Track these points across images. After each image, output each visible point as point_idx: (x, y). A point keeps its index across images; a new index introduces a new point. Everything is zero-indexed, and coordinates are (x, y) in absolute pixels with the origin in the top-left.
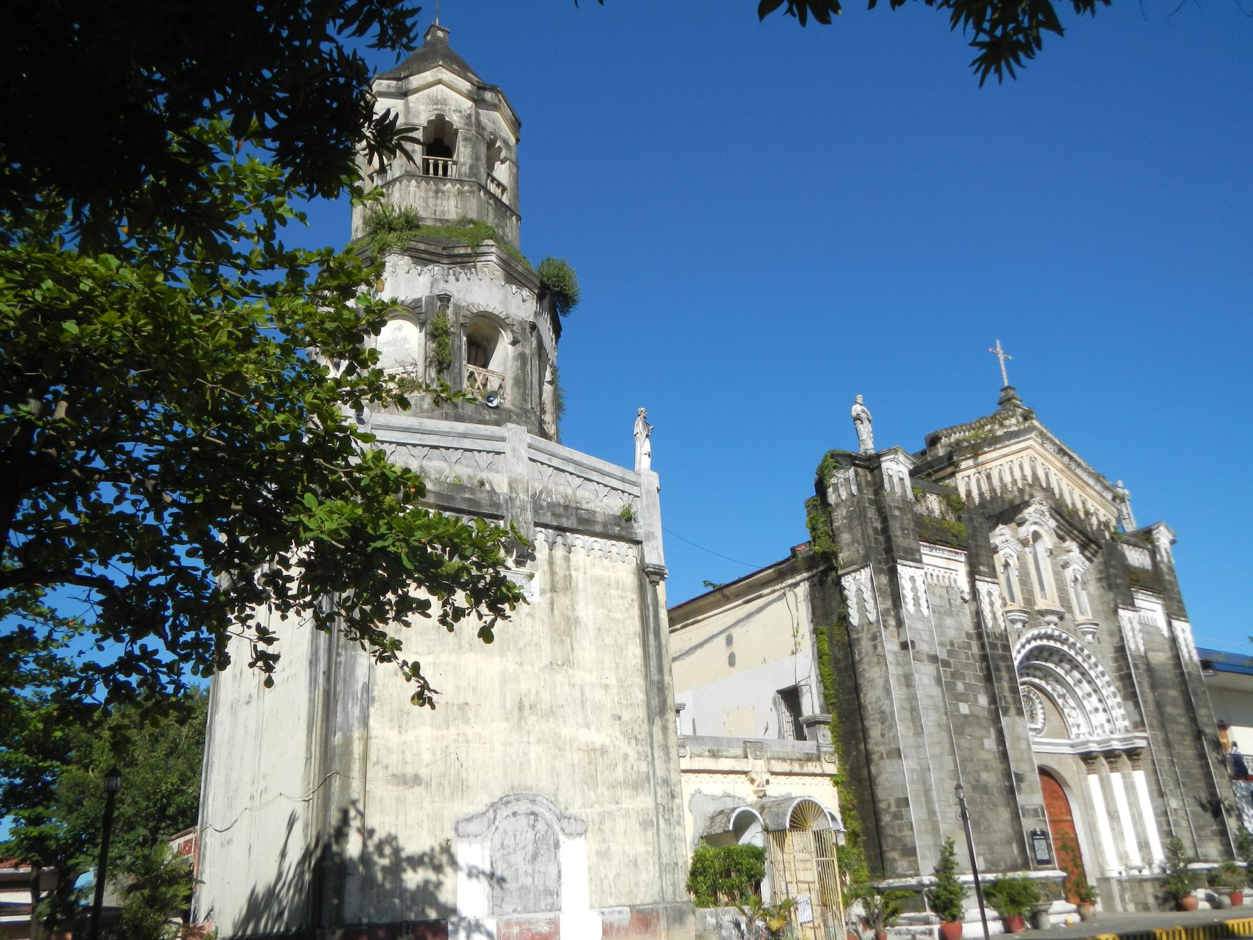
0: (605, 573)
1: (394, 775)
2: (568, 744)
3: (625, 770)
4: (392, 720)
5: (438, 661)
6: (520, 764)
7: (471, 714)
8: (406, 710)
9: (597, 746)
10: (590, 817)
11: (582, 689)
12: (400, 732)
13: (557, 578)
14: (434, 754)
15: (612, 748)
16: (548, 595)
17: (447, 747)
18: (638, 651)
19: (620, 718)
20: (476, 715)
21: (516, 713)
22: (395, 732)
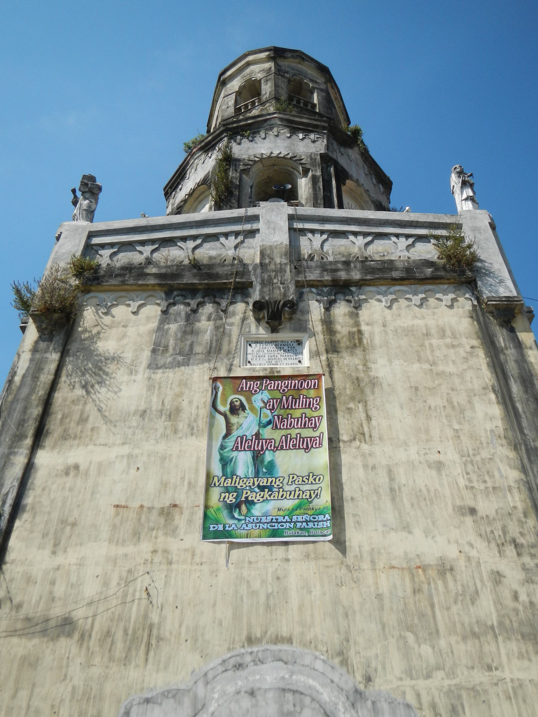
0: (416, 322)
1: (28, 619)
2: (367, 557)
3: (498, 602)
4: (45, 535)
5: (136, 451)
6: (268, 597)
7: (180, 521)
8: (71, 520)
9: (431, 559)
10: (425, 700)
11: (390, 472)
12: (54, 553)
13: (338, 336)
14: (106, 584)
15: (462, 563)
16: (324, 358)
17: (130, 571)
18: (497, 410)
19: (473, 511)
22: (47, 552)
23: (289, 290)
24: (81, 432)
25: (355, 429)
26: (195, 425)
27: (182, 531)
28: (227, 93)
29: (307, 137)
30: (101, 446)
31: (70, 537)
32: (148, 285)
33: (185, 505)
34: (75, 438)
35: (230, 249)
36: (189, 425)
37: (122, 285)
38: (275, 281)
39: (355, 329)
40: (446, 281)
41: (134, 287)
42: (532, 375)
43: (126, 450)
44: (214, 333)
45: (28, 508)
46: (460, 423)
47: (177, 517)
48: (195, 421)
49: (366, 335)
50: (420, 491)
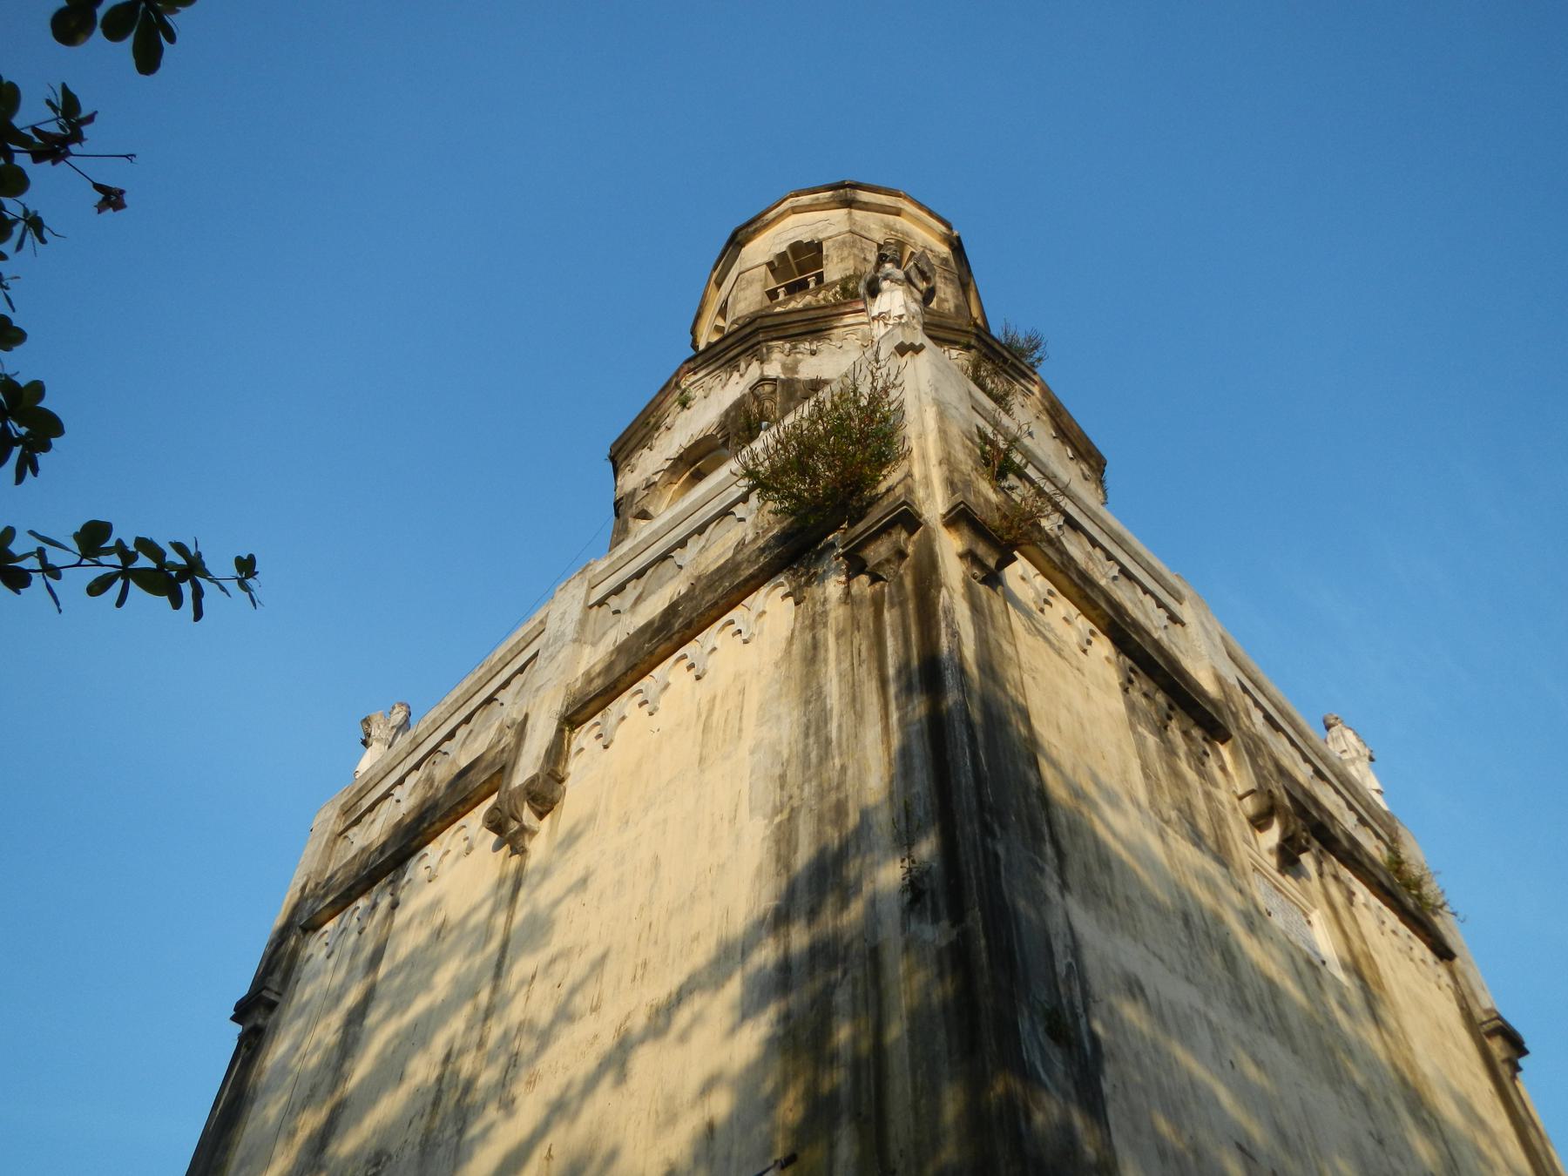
28: (857, 229)
37: (1061, 572)
41: (1072, 591)
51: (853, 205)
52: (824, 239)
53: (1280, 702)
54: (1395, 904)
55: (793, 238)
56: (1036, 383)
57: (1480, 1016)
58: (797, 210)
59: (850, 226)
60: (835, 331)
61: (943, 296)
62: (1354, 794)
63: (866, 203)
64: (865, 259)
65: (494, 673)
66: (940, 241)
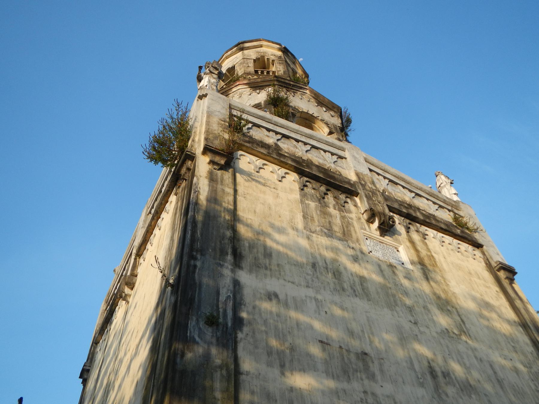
5: (319, 297)
11: (491, 366)
20: (382, 371)
21: (429, 377)
23: (385, 208)
24: (270, 264)
25: (459, 327)
26: (355, 289)
27: (379, 377)
28: (245, 57)
29: (328, 111)
30: (290, 283)
31: (292, 361)
32: (287, 164)
33: (373, 356)
34: (266, 268)
35: (331, 163)
36: (352, 288)
37: (268, 156)
38: (374, 199)
39: (429, 253)
40: (467, 242)
41: (276, 161)
42: (536, 322)
43: (311, 292)
44: (342, 220)
45: (245, 322)
46: (513, 342)
47: (371, 365)
48: (354, 285)
49: (437, 260)
50: (514, 386)
51: (244, 49)
52: (236, 64)
53: (397, 174)
54: (450, 234)
55: (228, 66)
56: (307, 89)
57: (494, 264)
58: (228, 57)
59: (243, 57)
60: (230, 95)
61: (279, 70)
62: (437, 198)
63: (248, 47)
64: (248, 66)
65: (132, 245)
66: (278, 51)
